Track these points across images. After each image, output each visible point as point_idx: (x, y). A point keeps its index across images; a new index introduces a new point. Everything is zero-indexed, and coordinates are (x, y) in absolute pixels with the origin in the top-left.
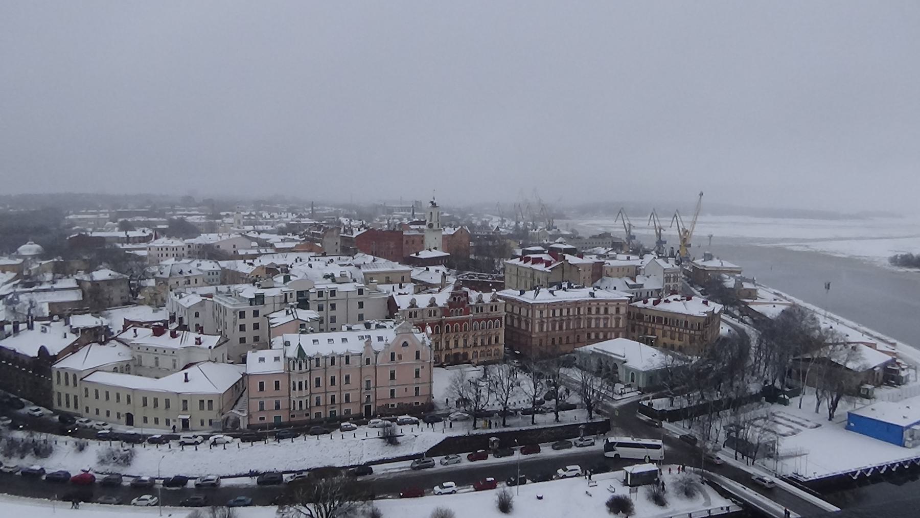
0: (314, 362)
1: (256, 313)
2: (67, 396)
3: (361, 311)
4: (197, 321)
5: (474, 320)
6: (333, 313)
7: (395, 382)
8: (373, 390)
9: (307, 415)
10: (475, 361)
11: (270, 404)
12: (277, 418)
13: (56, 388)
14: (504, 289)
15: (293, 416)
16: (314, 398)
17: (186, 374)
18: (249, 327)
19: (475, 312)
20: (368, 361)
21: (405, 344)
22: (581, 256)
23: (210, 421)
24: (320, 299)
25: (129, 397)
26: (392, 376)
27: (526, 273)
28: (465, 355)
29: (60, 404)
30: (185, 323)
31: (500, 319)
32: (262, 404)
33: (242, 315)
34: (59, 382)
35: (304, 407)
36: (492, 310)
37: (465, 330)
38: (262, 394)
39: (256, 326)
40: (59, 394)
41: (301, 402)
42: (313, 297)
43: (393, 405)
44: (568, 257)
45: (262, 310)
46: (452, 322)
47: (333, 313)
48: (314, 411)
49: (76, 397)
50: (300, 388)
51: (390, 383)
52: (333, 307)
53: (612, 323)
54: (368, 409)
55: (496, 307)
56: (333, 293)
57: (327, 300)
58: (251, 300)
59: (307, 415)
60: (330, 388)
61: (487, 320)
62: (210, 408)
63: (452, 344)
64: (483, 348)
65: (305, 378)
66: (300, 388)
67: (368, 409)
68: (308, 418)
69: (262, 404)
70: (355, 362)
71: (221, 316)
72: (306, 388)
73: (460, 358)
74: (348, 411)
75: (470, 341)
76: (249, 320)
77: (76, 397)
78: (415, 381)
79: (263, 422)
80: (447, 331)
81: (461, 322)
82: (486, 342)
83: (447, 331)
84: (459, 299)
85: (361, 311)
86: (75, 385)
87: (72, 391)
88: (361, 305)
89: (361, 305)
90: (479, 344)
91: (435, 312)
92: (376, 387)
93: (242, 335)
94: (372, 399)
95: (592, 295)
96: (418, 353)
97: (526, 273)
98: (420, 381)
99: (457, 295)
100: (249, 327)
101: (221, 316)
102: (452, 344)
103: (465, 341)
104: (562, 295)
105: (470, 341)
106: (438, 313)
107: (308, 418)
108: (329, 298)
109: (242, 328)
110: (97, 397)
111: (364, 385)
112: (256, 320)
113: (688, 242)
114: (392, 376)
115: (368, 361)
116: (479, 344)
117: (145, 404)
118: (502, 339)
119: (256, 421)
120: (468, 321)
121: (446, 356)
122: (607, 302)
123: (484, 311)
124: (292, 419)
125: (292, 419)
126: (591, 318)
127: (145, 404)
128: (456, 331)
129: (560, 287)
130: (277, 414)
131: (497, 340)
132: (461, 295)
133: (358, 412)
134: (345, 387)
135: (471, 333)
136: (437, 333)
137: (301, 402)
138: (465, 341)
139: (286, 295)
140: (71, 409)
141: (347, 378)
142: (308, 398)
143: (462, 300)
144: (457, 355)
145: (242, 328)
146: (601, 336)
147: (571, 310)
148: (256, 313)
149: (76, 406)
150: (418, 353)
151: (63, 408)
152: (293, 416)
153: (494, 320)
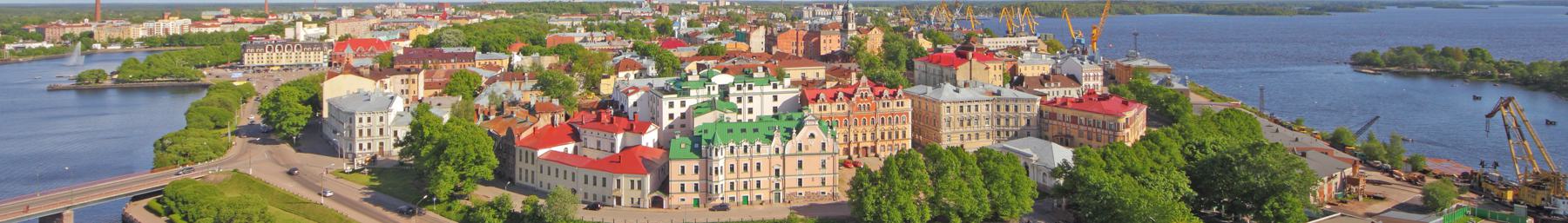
1: (683, 104)
11: (689, 187)
13: (519, 165)
21: (812, 136)
26: (800, 164)
28: (874, 149)
33: (671, 105)
42: (733, 90)
52: (751, 100)
56: (750, 87)
70: (765, 150)
88: (775, 98)
89: (775, 98)
105: (879, 136)
114: (800, 164)
118: (909, 134)
134: (756, 174)
135: (879, 127)
140: (529, 183)
148: (683, 104)
151: (523, 182)
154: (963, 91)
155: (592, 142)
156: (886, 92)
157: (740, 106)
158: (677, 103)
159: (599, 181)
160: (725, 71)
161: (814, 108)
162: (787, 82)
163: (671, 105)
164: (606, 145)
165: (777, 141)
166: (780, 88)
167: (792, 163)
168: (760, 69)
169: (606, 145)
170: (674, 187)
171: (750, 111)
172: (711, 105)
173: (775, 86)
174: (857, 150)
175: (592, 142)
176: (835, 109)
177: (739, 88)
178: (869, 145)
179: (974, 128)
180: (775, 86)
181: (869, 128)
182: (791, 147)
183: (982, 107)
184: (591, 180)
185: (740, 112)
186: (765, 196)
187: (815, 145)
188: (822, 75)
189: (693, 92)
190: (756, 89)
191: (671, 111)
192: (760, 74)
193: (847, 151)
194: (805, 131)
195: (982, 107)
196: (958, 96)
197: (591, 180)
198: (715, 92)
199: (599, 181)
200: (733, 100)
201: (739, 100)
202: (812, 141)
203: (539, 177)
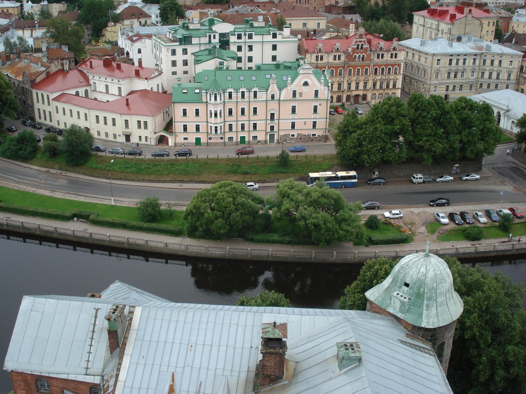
0: (227, 95)
1: (185, 52)
2: (44, 111)
3: (274, 53)
4: (139, 56)
5: (374, 66)
6: (250, 54)
7: (295, 116)
8: (276, 121)
9: (222, 138)
10: (373, 102)
11: (191, 128)
12: (198, 140)
14: (410, 38)
15: (210, 139)
16: (227, 124)
17: (127, 100)
18: (180, 63)
19: (376, 59)
20: (273, 97)
21: (306, 84)
22: (487, 11)
23: (146, 137)
24: (239, 41)
25: (86, 114)
26: (294, 110)
27: (432, 24)
28: (364, 97)
29: (40, 118)
30: (131, 57)
31: (399, 65)
32: (185, 128)
33: (174, 52)
34: (38, 101)
35: (219, 132)
36: (392, 57)
37: (366, 73)
38: (185, 119)
39: (185, 63)
40: (39, 109)
41: (216, 127)
42: (233, 39)
43: (293, 135)
44: (473, 9)
45: (191, 49)
46: (354, 67)
47: (250, 54)
48: (228, 135)
49: (50, 112)
50: (216, 115)
51: (292, 116)
52: (251, 48)
53: (504, 76)
54: (272, 137)
55: (396, 54)
56: (250, 37)
57: (245, 42)
58: (180, 39)
59: (222, 138)
60: (241, 118)
61: (386, 65)
62: (146, 127)
63: (353, 87)
64: (381, 92)
65: (219, 109)
66: (216, 115)
67: (272, 137)
68: (222, 141)
69: (185, 128)
70: (262, 96)
71: (158, 52)
72: (221, 116)
73: (360, 99)
74: (255, 137)
75: (370, 85)
76: (180, 57)
77: (50, 112)
78: (314, 116)
79: (186, 141)
80: (350, 74)
81: (362, 67)
82: (384, 86)
83: (350, 74)
84: (362, 45)
85: (274, 53)
86: (49, 104)
87: (48, 109)
88: (274, 48)
89: (274, 48)
90: (378, 86)
91: (339, 56)
92: (279, 119)
93: (174, 69)
94: (276, 129)
95: (488, 48)
96: (316, 92)
97: (432, 24)
98: (317, 116)
99: (360, 42)
100: (180, 63)
101: (158, 52)
102: (353, 87)
103: (366, 84)
104: (458, 48)
105: (370, 85)
106: (343, 58)
107: (222, 141)
108: (247, 40)
109: (174, 64)
110: (64, 114)
111: (269, 117)
112: (185, 57)
113: (23, 55)
114: (294, 110)
115: (273, 97)
116: (378, 86)
117: (98, 122)
118: (399, 85)
119: (180, 139)
120: (369, 66)
121: (347, 96)
122: (501, 55)
123: (385, 58)
124: (210, 141)
125: (210, 141)
126: (485, 70)
127: (98, 122)
128: (358, 74)
129: (459, 39)
130: (198, 135)
131: (394, 86)
132: (364, 42)
133: (264, 139)
134: (253, 117)
136: (340, 74)
137: (216, 127)
138: (366, 84)
139: (210, 36)
140: (48, 122)
141: (255, 110)
142: (222, 124)
143: (364, 46)
144: (357, 96)
145: (174, 64)
146: (493, 86)
147: (467, 61)
148: (185, 52)
149: (51, 121)
150: (316, 92)
152: (210, 139)
153: (393, 65)
154: (455, 44)
155: (101, 87)
156: (382, 43)
157: (240, 54)
158: (179, 50)
159: (110, 122)
160: (225, 20)
161: (311, 58)
162: (286, 32)
163: (174, 52)
164: (114, 90)
165: (273, 89)
166: (279, 38)
167: (286, 109)
168: (261, 18)
169: (114, 90)
170: (178, 127)
171: (250, 59)
172: (211, 53)
173: (274, 36)
174: (348, 98)
175: (101, 87)
176: (331, 59)
177: (239, 37)
178: (361, 93)
179: (459, 80)
180: (274, 36)
181: (362, 78)
182: (286, 94)
183: (469, 61)
184: (101, 120)
185: (239, 60)
186: (261, 137)
187: (308, 92)
188: (323, 26)
189: (195, 41)
190: (255, 38)
191: (174, 58)
192: (260, 22)
193: (339, 99)
194: (300, 80)
195: (469, 61)
196: (450, 50)
197: (101, 120)
198: (216, 41)
199: (110, 122)
200: (233, 48)
201: (239, 49)
202: (305, 89)
203: (56, 117)
